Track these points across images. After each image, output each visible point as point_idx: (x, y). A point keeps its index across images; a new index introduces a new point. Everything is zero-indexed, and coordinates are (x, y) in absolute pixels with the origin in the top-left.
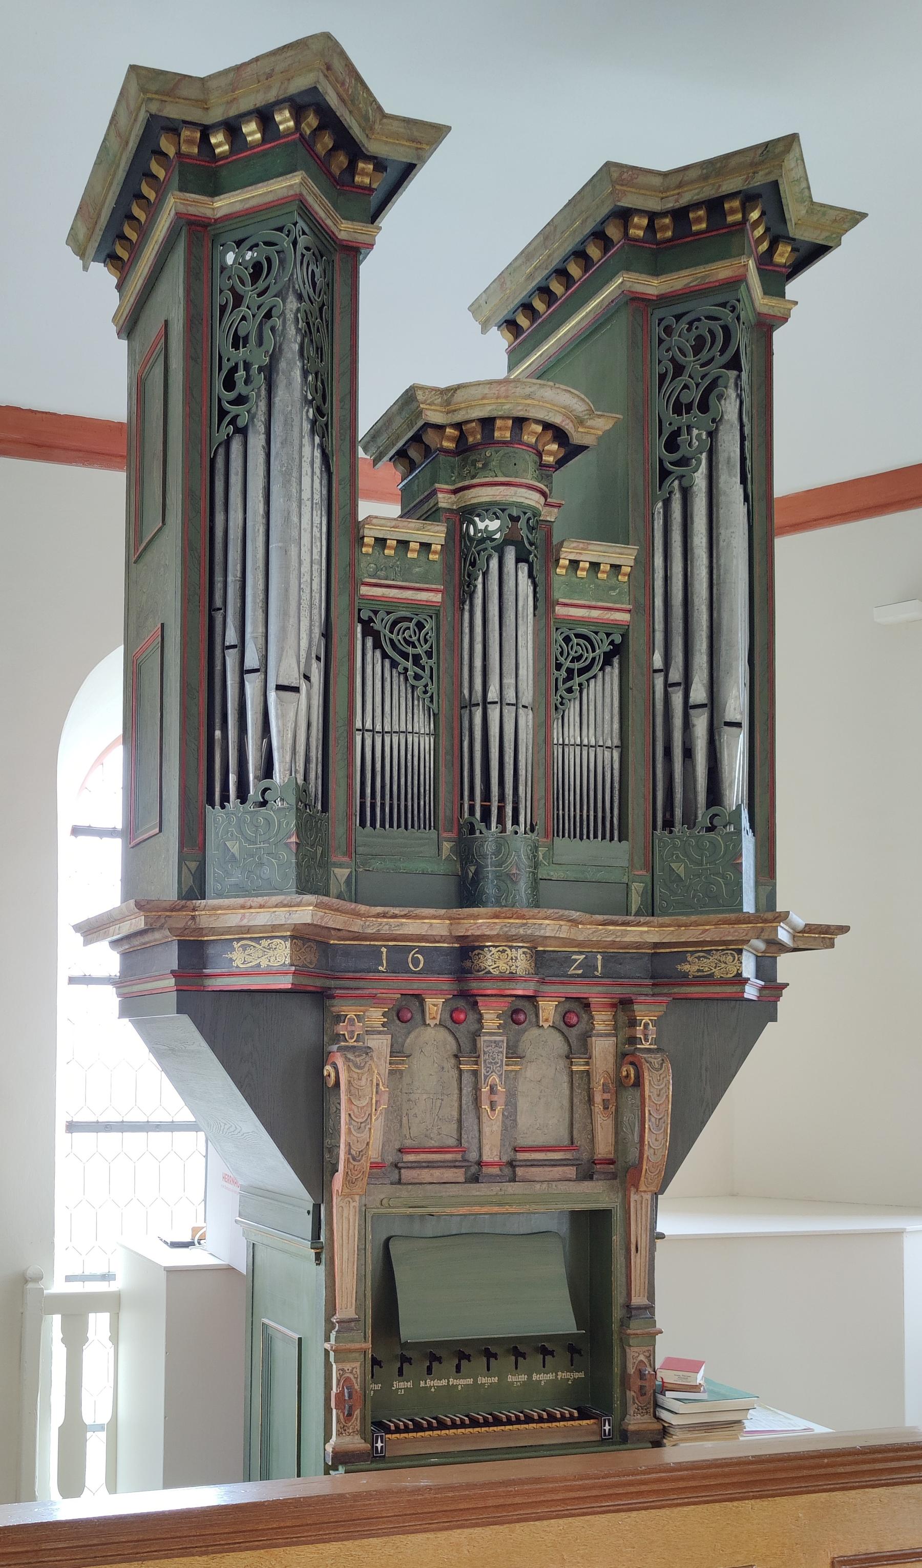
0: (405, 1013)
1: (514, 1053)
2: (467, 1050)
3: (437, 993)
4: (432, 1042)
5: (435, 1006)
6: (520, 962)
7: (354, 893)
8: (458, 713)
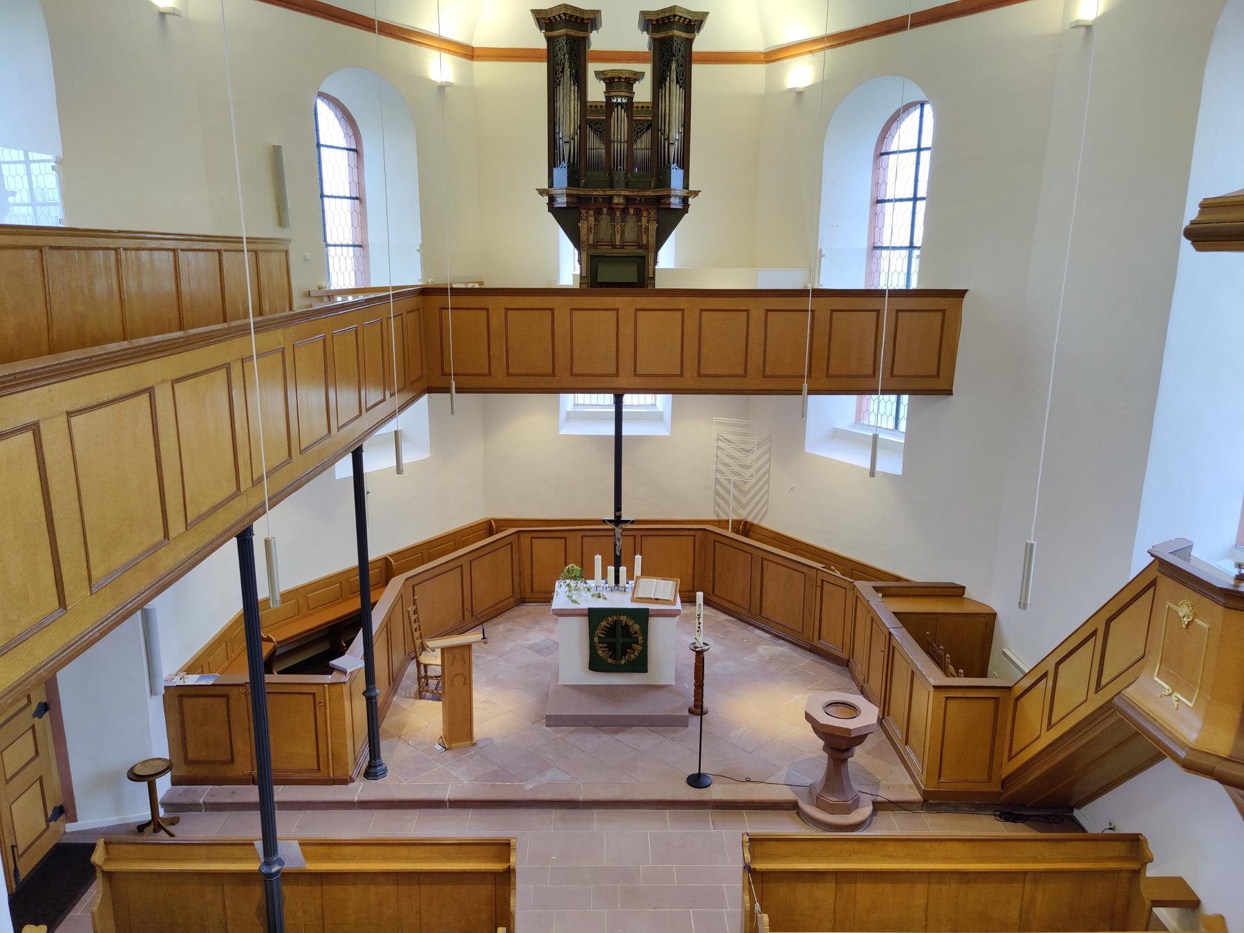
0: (598, 212)
1: (623, 220)
2: (613, 220)
4: (605, 219)
5: (605, 210)
6: (621, 200)
7: (586, 186)
8: (608, 143)
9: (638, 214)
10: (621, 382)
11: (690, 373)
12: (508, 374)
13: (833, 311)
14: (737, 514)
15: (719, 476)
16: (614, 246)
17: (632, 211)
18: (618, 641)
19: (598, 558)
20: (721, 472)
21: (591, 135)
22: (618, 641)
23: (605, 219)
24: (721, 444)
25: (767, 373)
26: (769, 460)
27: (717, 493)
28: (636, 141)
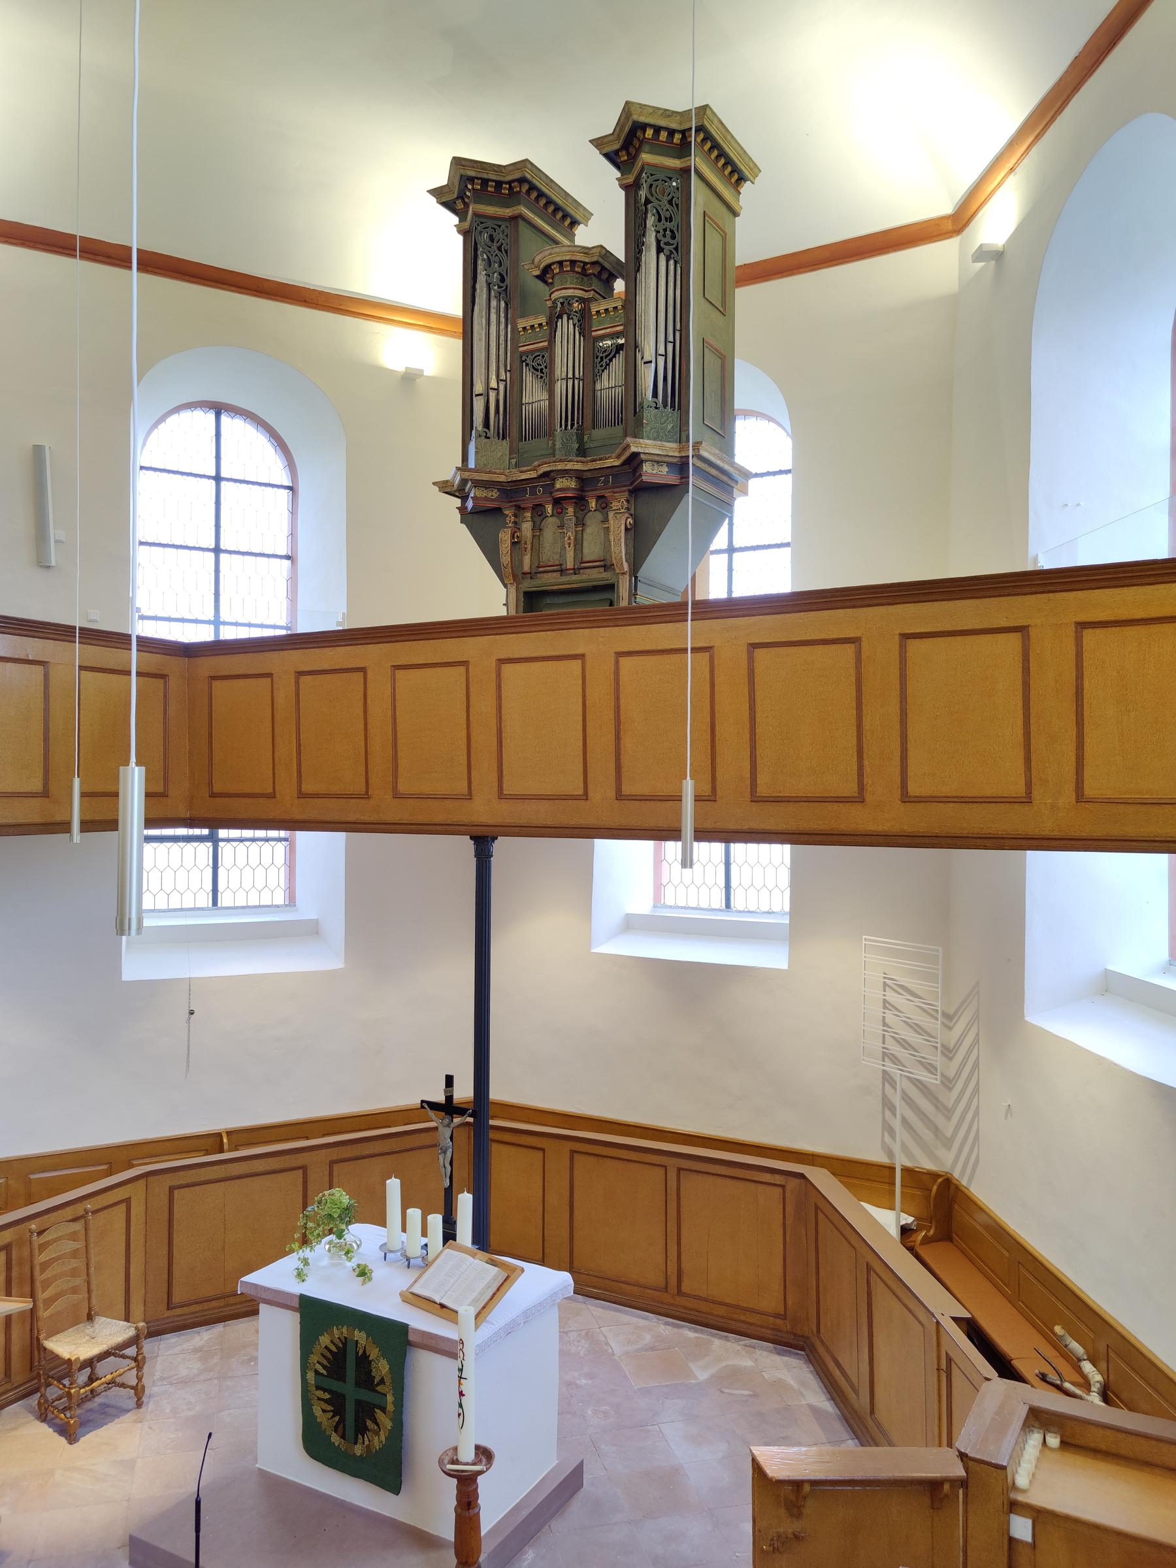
3: (548, 502)
9: (604, 504)
10: (483, 810)
11: (603, 791)
12: (301, 795)
13: (905, 637)
14: (932, 1156)
15: (891, 1068)
16: (562, 571)
17: (593, 504)
18: (357, 1385)
19: (394, 1186)
20: (895, 1060)
21: (529, 377)
22: (357, 1385)
23: (551, 524)
24: (892, 997)
25: (762, 790)
26: (976, 1041)
27: (888, 1104)
28: (596, 376)
